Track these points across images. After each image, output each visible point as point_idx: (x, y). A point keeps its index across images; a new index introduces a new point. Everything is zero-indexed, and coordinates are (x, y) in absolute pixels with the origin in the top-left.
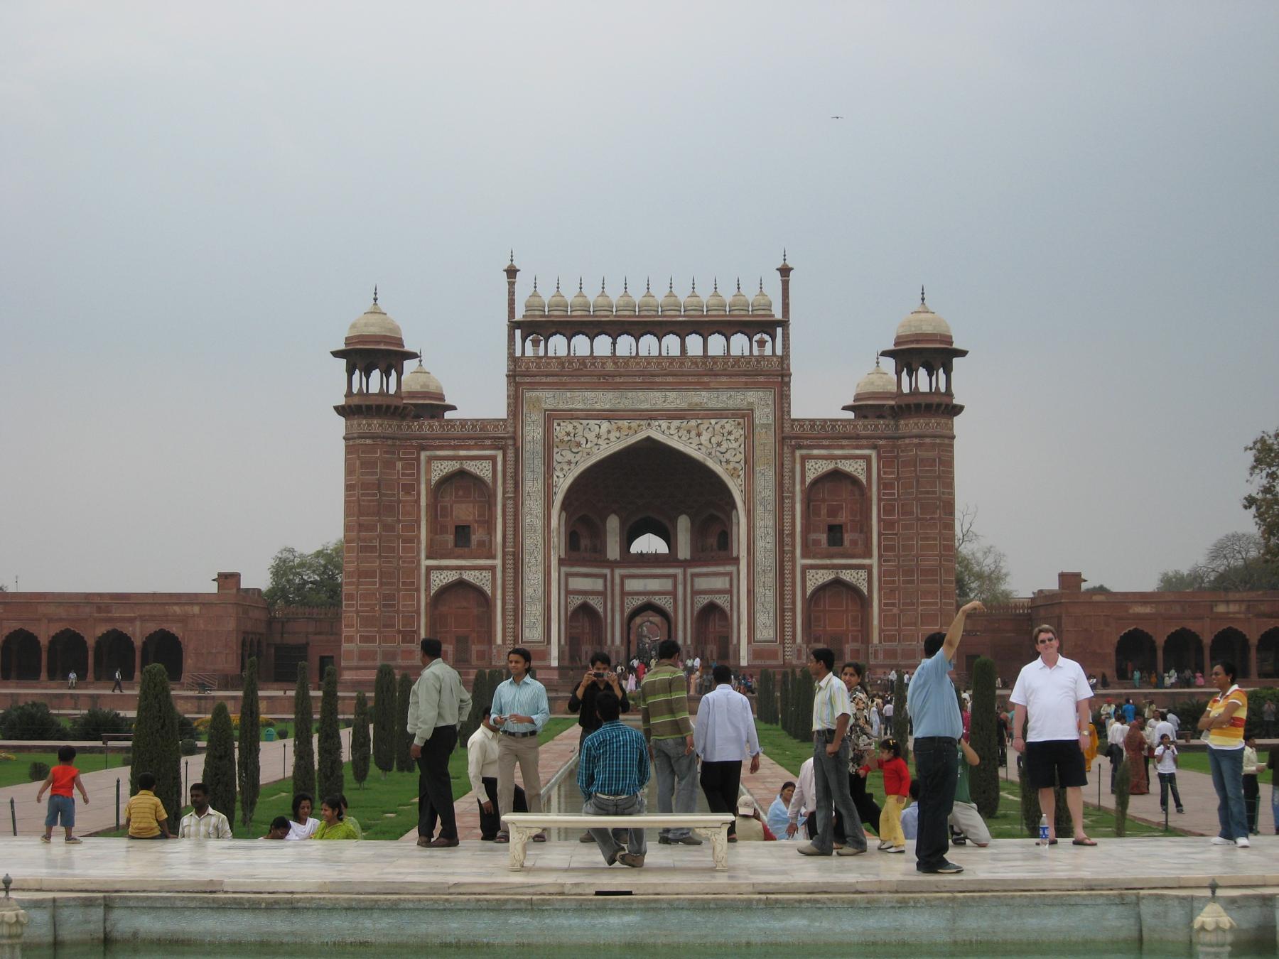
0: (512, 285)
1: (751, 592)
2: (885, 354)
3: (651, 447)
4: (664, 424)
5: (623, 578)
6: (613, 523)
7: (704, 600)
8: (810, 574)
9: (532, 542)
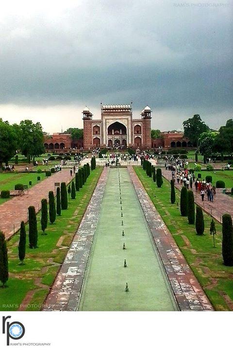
3: (117, 123)
6: (113, 130)
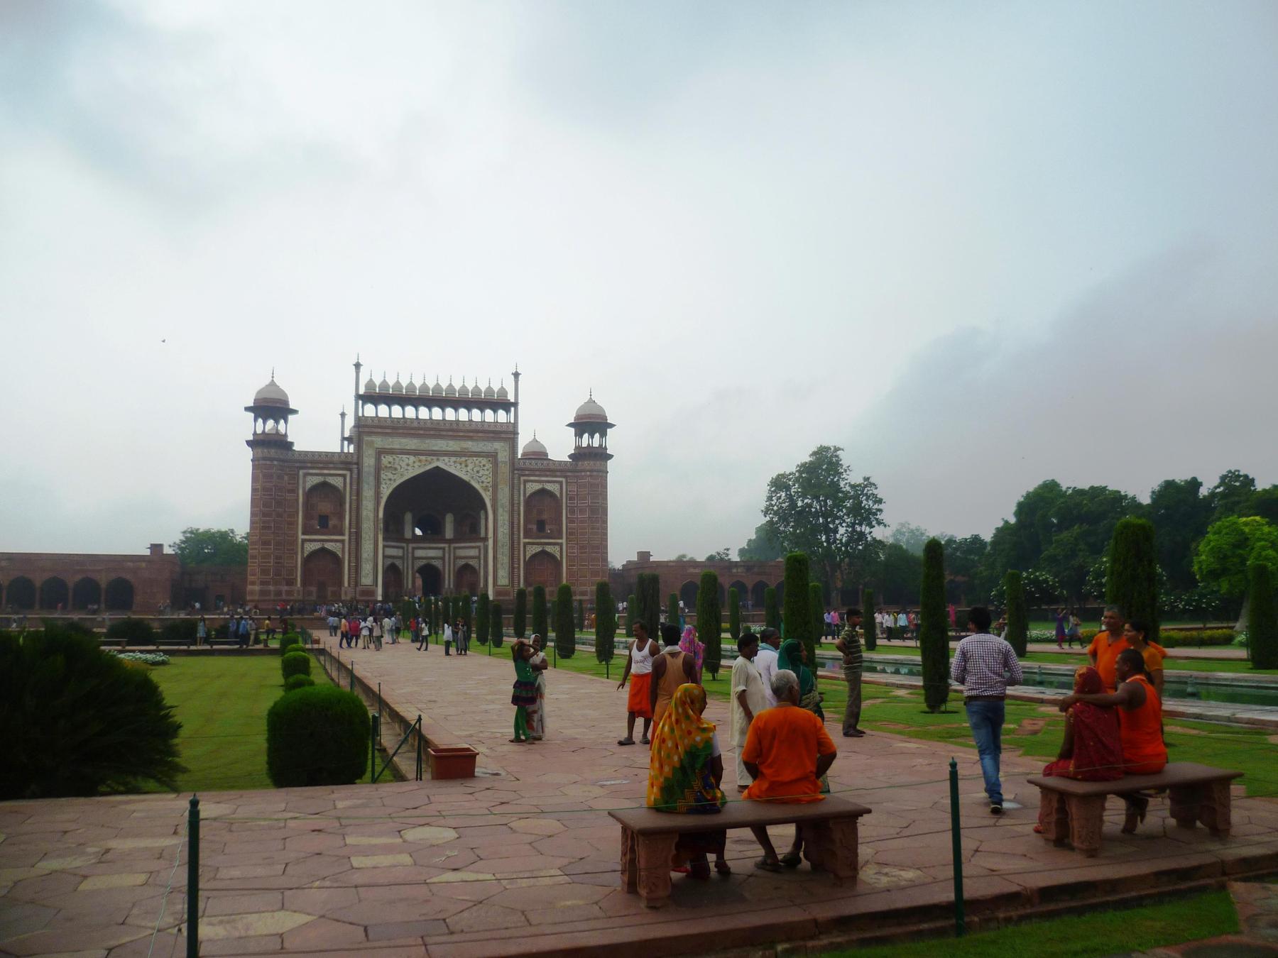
1: (495, 558)
2: (570, 425)
4: (446, 459)
5: (414, 549)
6: (408, 517)
7: (462, 562)
8: (528, 547)
9: (368, 527)
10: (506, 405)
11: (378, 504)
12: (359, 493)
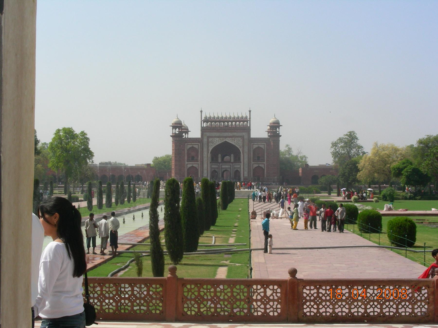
0: (201, 114)
6: (220, 155)
7: (236, 169)
9: (205, 159)
10: (247, 121)
11: (208, 152)
12: (202, 149)
